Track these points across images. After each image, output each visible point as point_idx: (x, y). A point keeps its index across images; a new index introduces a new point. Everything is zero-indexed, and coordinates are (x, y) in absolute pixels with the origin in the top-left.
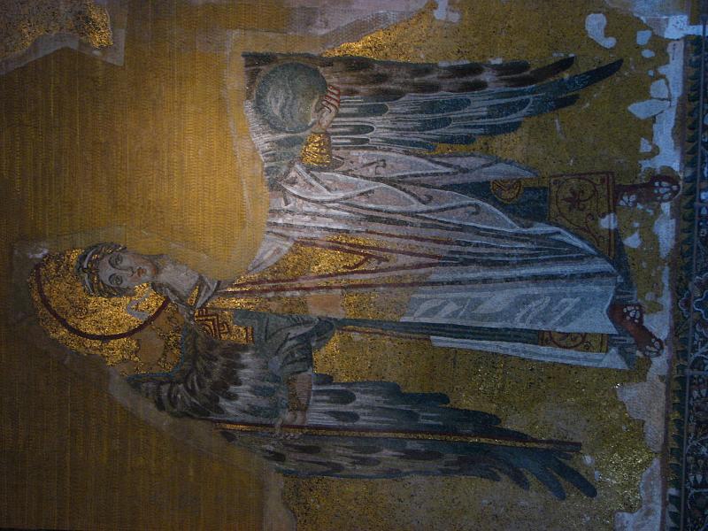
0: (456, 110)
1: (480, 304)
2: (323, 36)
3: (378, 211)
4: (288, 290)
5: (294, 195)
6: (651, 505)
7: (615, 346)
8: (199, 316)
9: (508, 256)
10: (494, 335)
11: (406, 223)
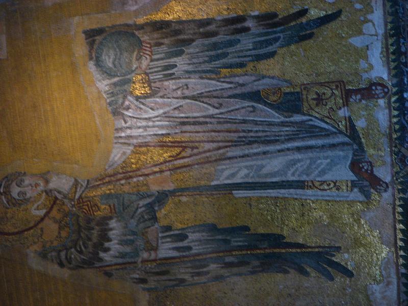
0: (231, 46)
1: (262, 168)
2: (135, 11)
3: (187, 118)
4: (135, 177)
5: (130, 117)
6: (390, 279)
7: (356, 187)
8: (78, 203)
9: (278, 136)
10: (275, 186)
11: (206, 123)
